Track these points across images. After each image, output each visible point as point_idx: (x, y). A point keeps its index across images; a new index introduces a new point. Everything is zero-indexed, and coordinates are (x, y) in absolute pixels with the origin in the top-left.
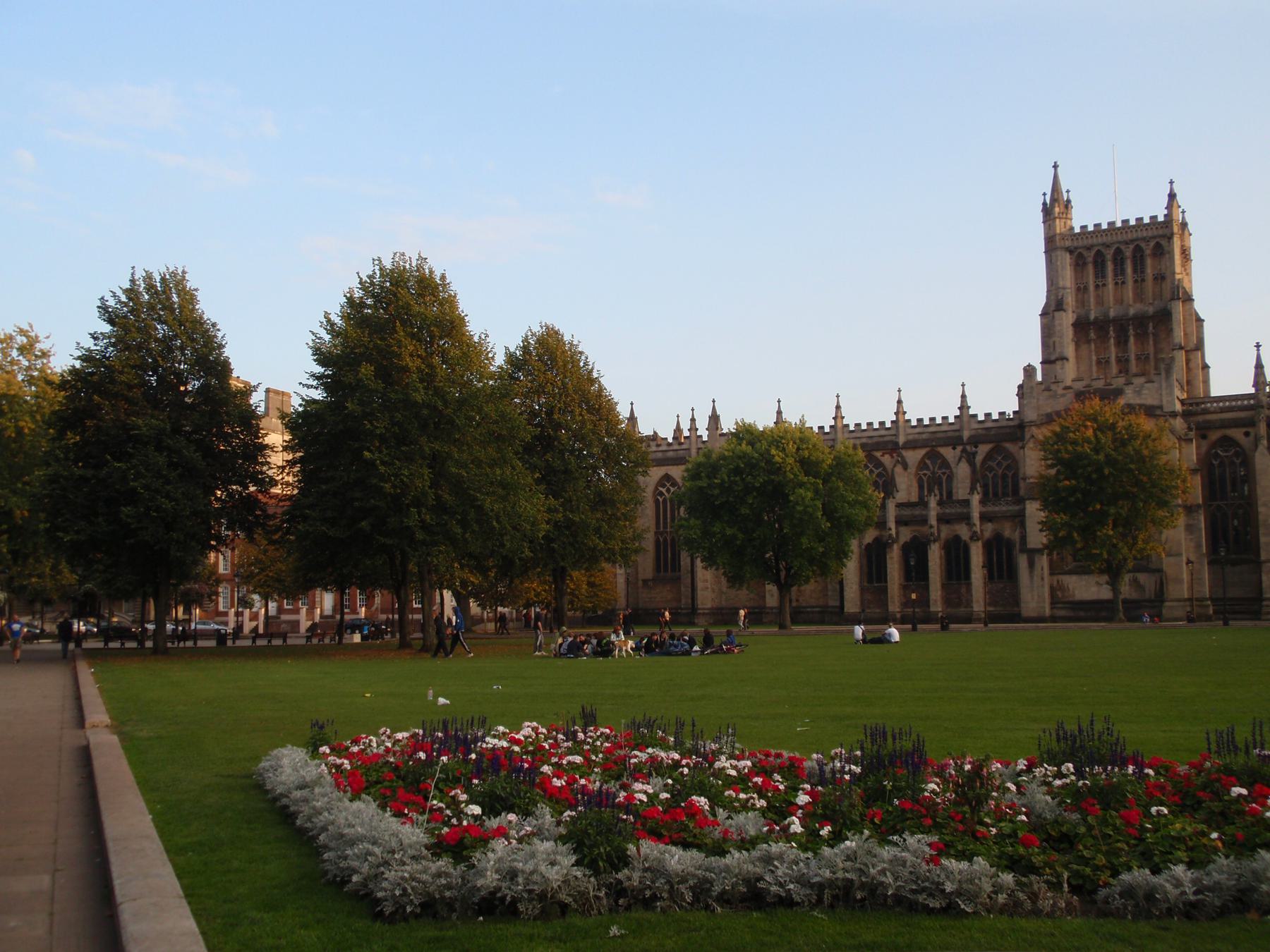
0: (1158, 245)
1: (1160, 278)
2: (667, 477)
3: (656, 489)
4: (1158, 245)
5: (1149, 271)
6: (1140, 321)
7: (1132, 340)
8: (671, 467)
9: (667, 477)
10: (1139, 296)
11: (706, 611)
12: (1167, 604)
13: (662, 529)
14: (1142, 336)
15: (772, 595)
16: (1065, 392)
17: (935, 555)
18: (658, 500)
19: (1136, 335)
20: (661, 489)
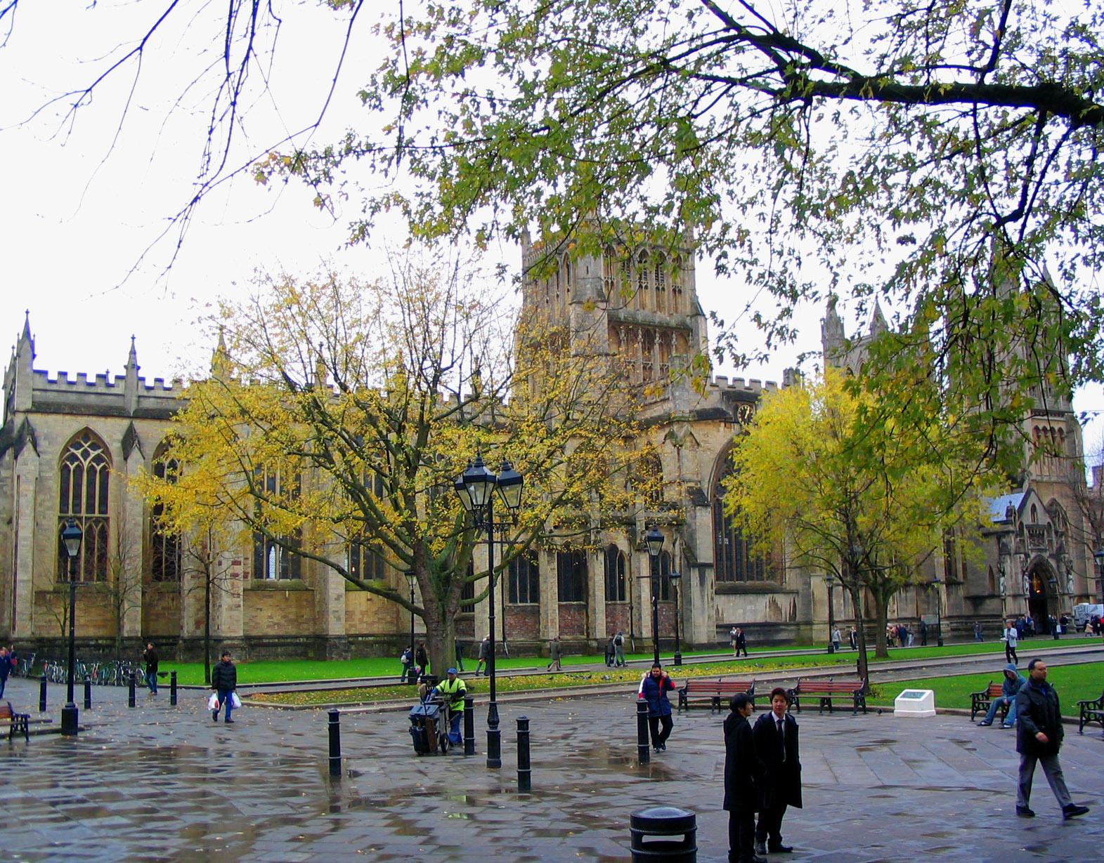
0: (678, 258)
1: (677, 291)
2: (87, 433)
3: (66, 449)
4: (678, 258)
5: (669, 283)
6: (666, 332)
7: (657, 347)
8: (94, 419)
9: (87, 433)
10: (660, 306)
11: (236, 642)
12: (815, 627)
13: (70, 513)
14: (666, 345)
15: (339, 619)
16: (712, 389)
17: (597, 570)
18: (67, 466)
19: (661, 345)
20: (73, 450)
